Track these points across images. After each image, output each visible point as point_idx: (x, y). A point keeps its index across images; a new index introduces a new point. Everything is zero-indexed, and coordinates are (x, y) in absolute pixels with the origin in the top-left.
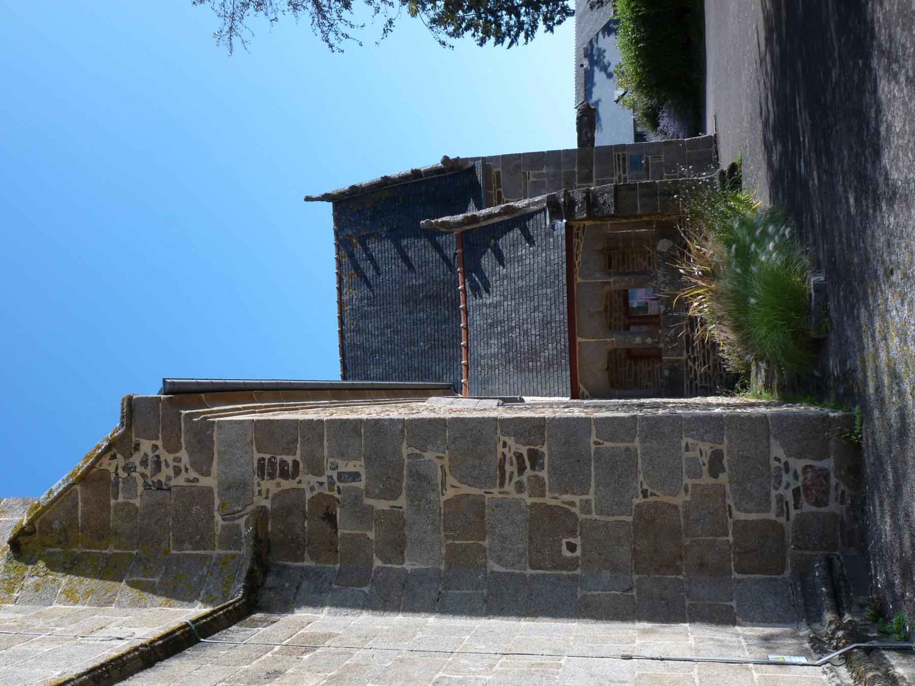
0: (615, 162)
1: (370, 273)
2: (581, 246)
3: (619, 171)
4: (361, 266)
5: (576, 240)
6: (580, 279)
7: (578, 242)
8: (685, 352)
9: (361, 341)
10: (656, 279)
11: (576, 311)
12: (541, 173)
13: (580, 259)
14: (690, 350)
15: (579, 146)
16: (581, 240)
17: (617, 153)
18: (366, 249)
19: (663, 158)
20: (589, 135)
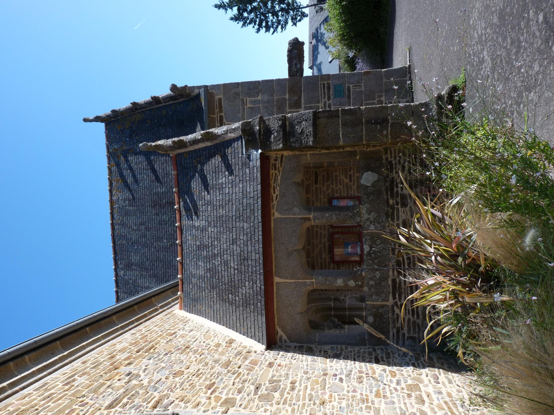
0: (321, 90)
1: (130, 180)
2: (279, 178)
3: (324, 98)
4: (124, 174)
5: (273, 171)
6: (279, 214)
7: (276, 174)
8: (391, 298)
9: (125, 233)
10: (360, 216)
11: (273, 249)
12: (256, 100)
13: (277, 192)
14: (397, 296)
15: (289, 76)
16: (279, 171)
17: (322, 82)
18: (127, 161)
19: (363, 87)
20: (298, 66)
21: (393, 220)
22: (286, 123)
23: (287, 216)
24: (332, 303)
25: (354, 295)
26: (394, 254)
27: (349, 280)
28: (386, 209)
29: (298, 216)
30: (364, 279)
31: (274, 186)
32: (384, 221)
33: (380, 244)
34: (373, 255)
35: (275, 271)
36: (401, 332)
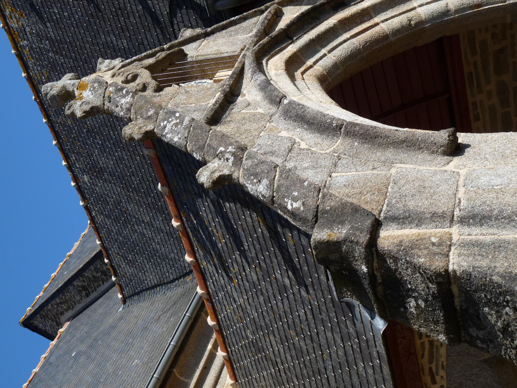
22: (451, 291)
31: (431, 369)
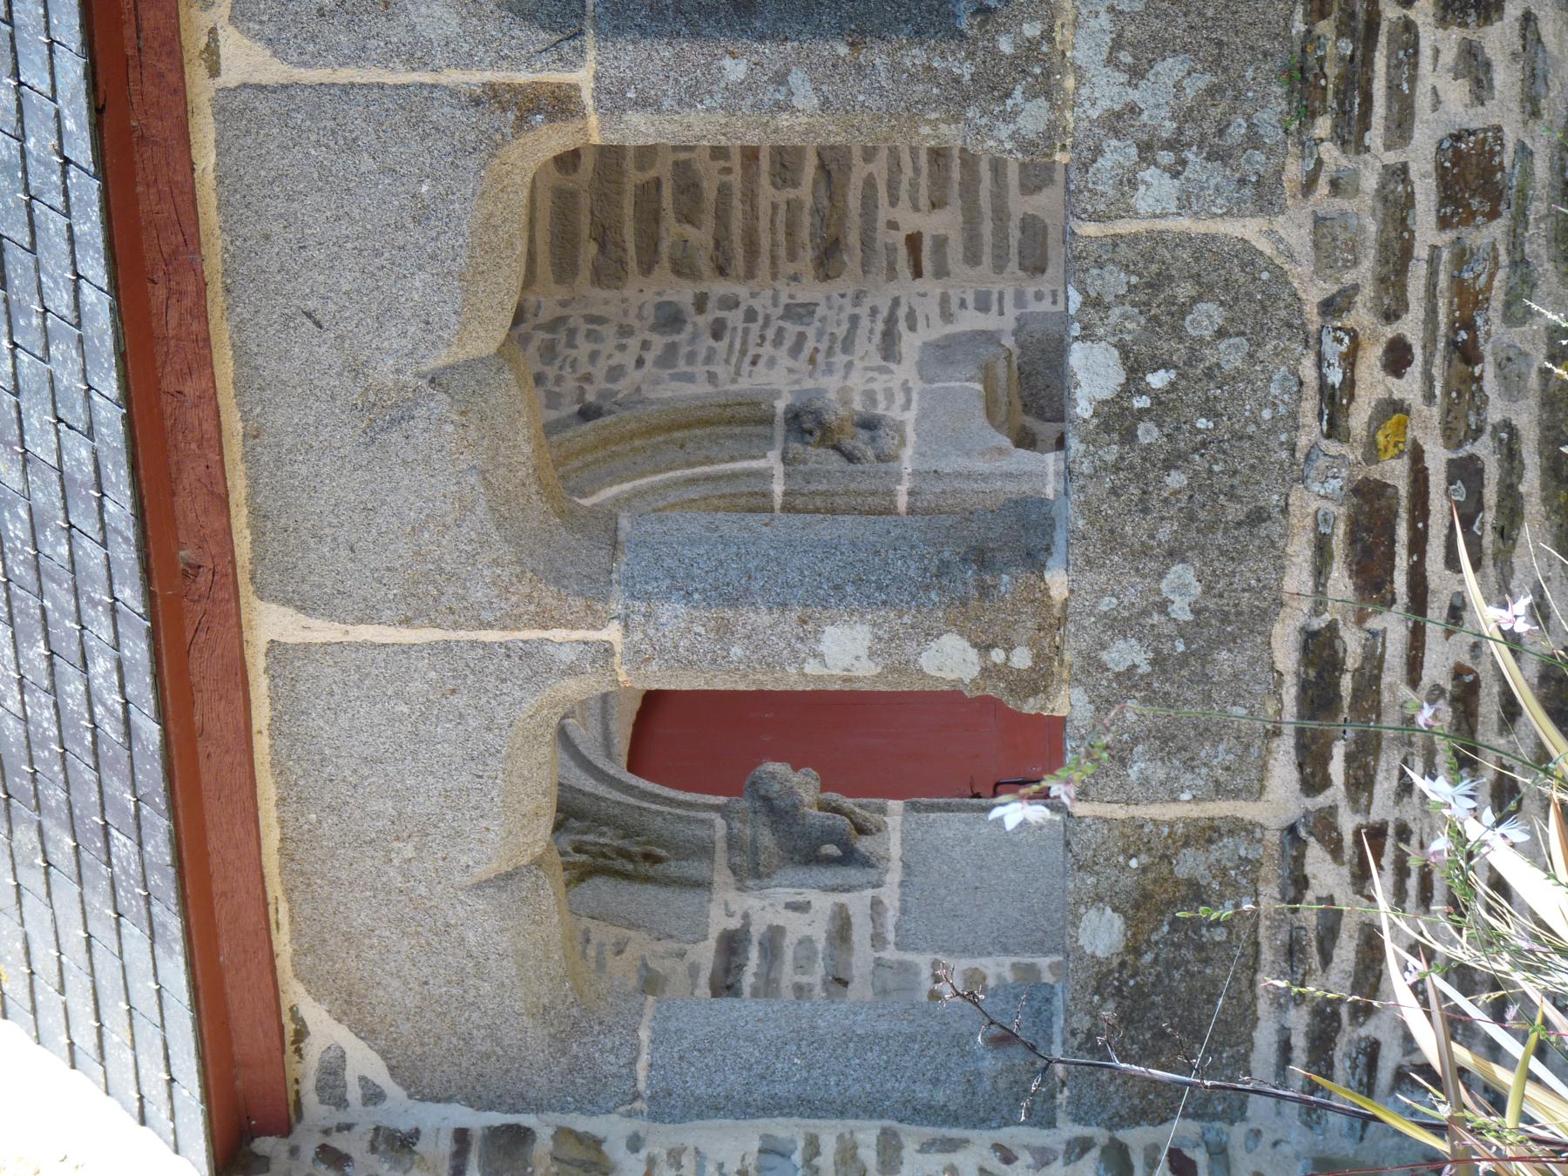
6: (261, 53)
10: (1046, 89)
14: (1337, 768)
21: (1351, 134)
23: (345, 75)
24: (772, 461)
25: (970, 321)
26: (1335, 429)
27: (931, 635)
28: (1299, 26)
29: (452, 77)
30: (1062, 621)
32: (1272, 135)
33: (1221, 333)
34: (1148, 433)
35: (258, 559)
36: (1348, 1037)
